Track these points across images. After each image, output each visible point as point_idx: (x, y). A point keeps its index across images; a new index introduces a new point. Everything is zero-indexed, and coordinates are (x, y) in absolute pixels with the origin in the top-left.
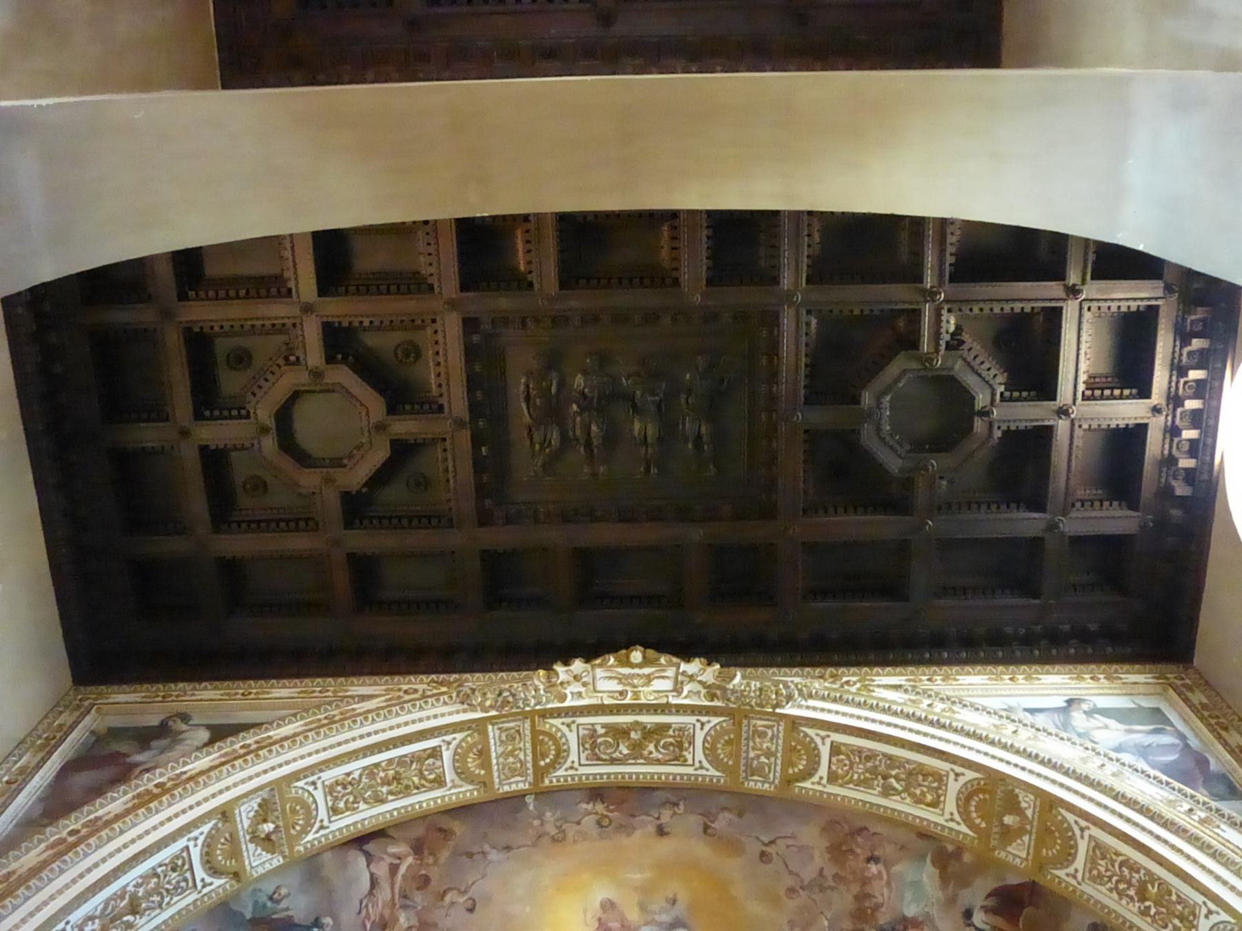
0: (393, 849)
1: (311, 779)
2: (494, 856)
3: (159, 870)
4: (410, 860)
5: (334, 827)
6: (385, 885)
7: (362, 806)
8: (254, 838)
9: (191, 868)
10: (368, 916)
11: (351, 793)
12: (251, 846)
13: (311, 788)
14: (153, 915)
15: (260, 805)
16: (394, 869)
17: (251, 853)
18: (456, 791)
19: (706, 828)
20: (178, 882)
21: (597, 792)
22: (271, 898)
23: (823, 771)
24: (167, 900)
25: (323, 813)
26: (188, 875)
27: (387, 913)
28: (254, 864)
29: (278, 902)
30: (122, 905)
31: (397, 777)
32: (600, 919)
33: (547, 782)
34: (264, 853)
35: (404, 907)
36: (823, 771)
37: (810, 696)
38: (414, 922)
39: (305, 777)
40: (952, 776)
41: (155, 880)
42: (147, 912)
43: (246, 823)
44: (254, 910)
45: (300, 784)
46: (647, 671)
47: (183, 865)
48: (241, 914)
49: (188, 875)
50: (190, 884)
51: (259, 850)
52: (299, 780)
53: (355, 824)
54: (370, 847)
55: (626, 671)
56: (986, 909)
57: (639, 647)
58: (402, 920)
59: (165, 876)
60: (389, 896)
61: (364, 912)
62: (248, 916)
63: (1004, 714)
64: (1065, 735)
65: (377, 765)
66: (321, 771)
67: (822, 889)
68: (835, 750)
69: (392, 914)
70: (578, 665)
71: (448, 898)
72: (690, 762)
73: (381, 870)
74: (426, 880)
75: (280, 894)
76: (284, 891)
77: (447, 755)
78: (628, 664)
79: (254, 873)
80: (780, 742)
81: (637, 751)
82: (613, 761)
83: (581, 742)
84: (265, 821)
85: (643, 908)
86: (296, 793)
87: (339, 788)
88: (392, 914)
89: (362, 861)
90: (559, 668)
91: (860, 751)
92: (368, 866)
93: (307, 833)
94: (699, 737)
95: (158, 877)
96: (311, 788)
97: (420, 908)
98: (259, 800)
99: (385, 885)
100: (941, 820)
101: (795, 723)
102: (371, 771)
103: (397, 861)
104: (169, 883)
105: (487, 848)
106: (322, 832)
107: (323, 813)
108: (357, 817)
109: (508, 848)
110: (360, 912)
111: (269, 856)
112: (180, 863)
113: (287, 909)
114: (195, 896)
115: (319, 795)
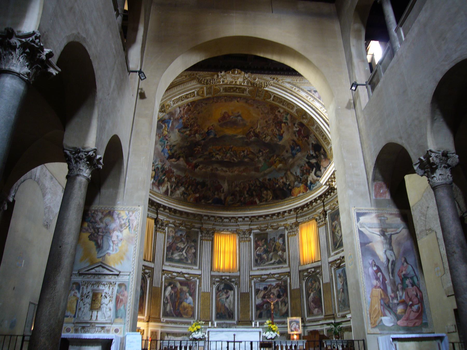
2: (203, 105)
4: (187, 107)
16: (184, 109)
18: (197, 98)
19: (246, 102)
21: (226, 96)
23: (272, 99)
25: (172, 105)
31: (186, 97)
32: (224, 115)
33: (215, 95)
35: (186, 114)
36: (272, 99)
37: (271, 85)
40: (296, 107)
46: (237, 75)
55: (233, 75)
56: (298, 125)
57: (237, 70)
63: (309, 92)
64: (319, 100)
65: (182, 96)
67: (268, 114)
68: (274, 96)
70: (223, 73)
71: (194, 112)
72: (245, 93)
73: (182, 109)
74: (190, 110)
77: (196, 92)
78: (233, 73)
80: (263, 95)
81: (234, 91)
82: (230, 92)
83: (223, 89)
85: (232, 113)
88: (184, 115)
90: (219, 74)
91: (279, 98)
94: (248, 90)
100: (292, 112)
101: (267, 91)
102: (181, 97)
105: (202, 104)
107: (172, 105)
108: (178, 104)
109: (206, 104)
115: (171, 103)
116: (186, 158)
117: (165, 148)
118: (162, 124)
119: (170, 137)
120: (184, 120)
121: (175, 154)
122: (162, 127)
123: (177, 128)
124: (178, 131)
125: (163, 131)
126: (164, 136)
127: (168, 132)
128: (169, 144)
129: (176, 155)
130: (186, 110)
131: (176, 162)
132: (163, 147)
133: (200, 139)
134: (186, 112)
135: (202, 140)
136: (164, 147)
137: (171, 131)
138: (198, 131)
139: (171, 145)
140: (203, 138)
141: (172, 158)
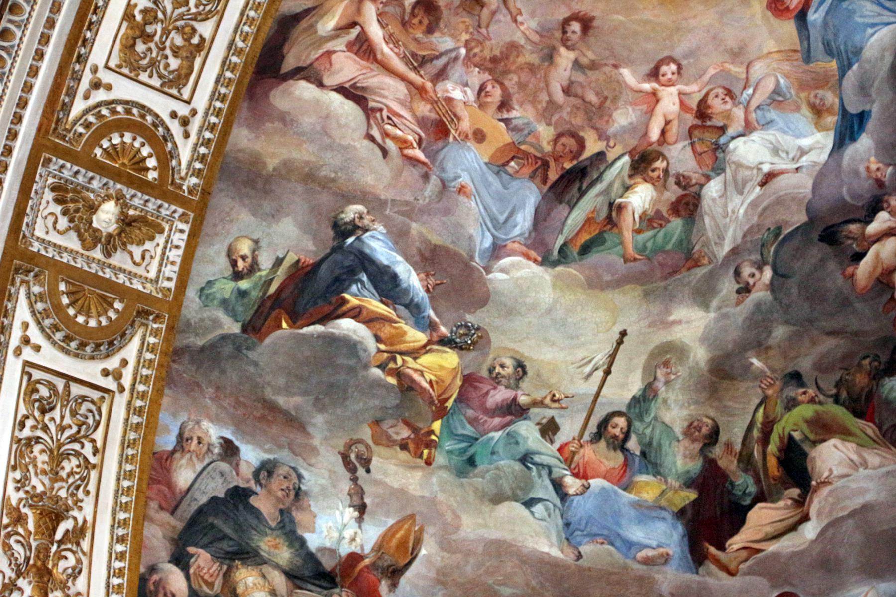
0: (328, 24)
1: (85, 84)
3: (27, 433)
5: (201, 101)
6: (376, 80)
7: (205, 29)
8: (110, 244)
9: (69, 378)
10: (403, 144)
11: (166, 33)
12: (119, 259)
13: (100, 95)
14: (92, 487)
15: (58, 201)
17: (129, 266)
20: (74, 414)
22: (238, 276)
24: (88, 450)
25: (161, 105)
26: (76, 390)
27: (424, 109)
28: (152, 274)
29: (254, 268)
30: (31, 526)
34: (148, 245)
35: (440, 75)
38: (476, 77)
39: (72, 93)
41: (37, 448)
42: (80, 494)
43: (72, 242)
44: (235, 316)
45: (78, 106)
47: (52, 386)
48: (224, 338)
49: (76, 390)
50: (95, 395)
51: (137, 251)
52: (67, 108)
53: (225, 63)
54: (290, 62)
58: (457, 94)
59: (45, 429)
60: (401, 89)
61: (390, 145)
62: (235, 328)
66: (82, 59)
69: (434, 102)
75: (244, 258)
76: (245, 248)
79: (167, 284)
84: (93, 209)
86: (87, 126)
87: (140, 47)
88: (434, 102)
89: (304, 89)
92: (320, 84)
93: (174, 154)
95: (38, 440)
96: (100, 95)
97: (463, 51)
98: (49, 195)
99: (376, 80)
103: (355, 32)
104: (62, 429)
106: (194, 128)
107: (161, 105)
110: (385, 152)
111: (160, 239)
112: (44, 391)
113: (279, 262)
114: (121, 401)
116: (858, 414)
117: (572, 484)
118: (318, 328)
119: (521, 367)
120: (479, 136)
121: (728, 464)
122: (351, 346)
123: (497, 250)
124: (546, 261)
125: (398, 373)
126: (462, 398)
127: (445, 342)
128: (569, 429)
129: (745, 460)
130: (390, 39)
131: (806, 518)
132: (543, 489)
133: (824, 157)
134: (419, 62)
135: (840, 144)
136: (558, 485)
137: (470, 319)
138: (717, 105)
139: (604, 424)
140: (831, 120)
141: (742, 522)
